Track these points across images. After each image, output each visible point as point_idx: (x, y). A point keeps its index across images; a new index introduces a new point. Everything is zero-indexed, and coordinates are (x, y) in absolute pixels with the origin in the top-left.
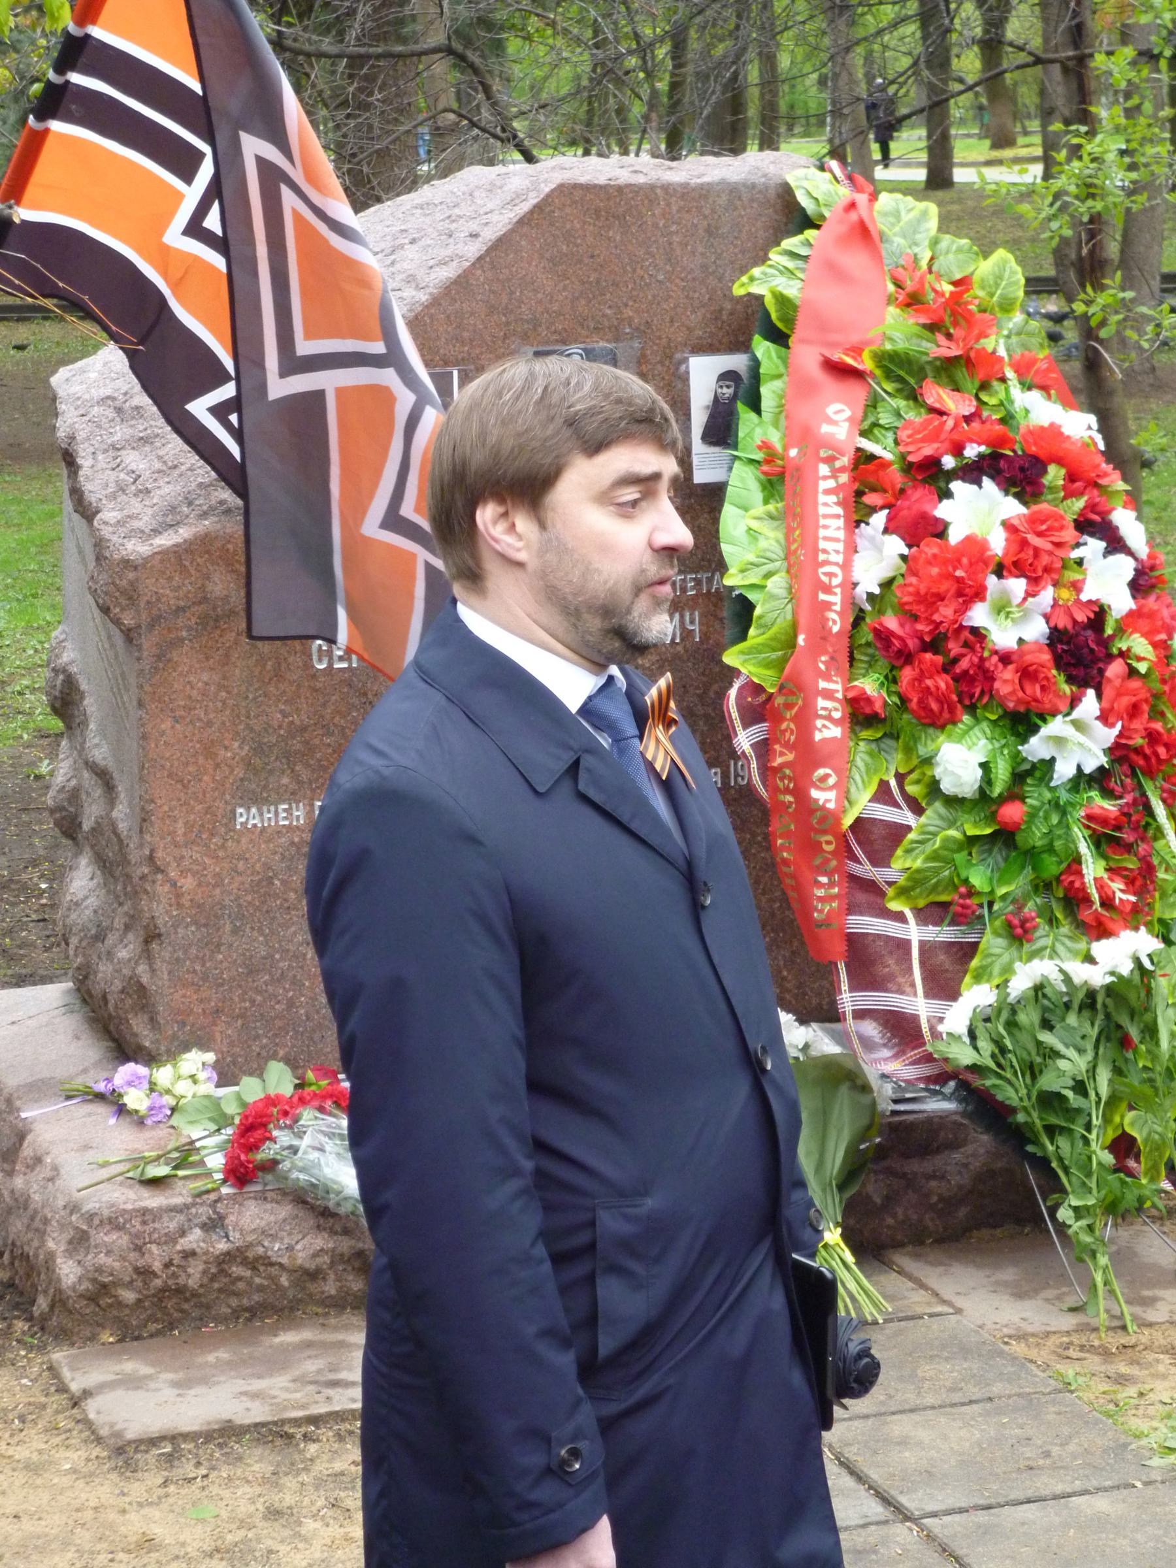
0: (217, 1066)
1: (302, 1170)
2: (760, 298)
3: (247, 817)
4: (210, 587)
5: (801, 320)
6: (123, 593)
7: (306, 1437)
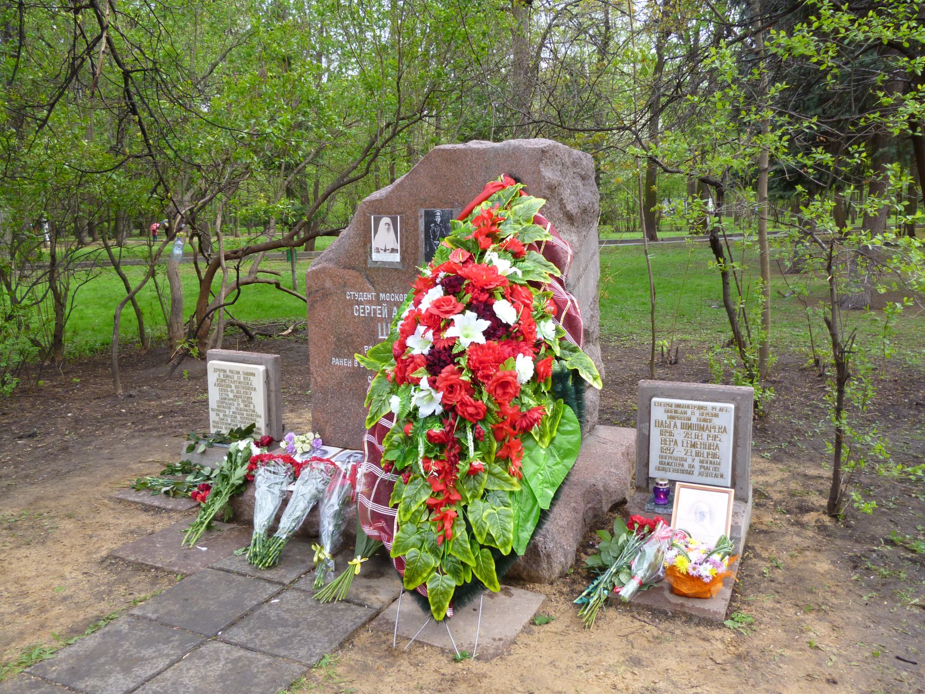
3: (336, 361)
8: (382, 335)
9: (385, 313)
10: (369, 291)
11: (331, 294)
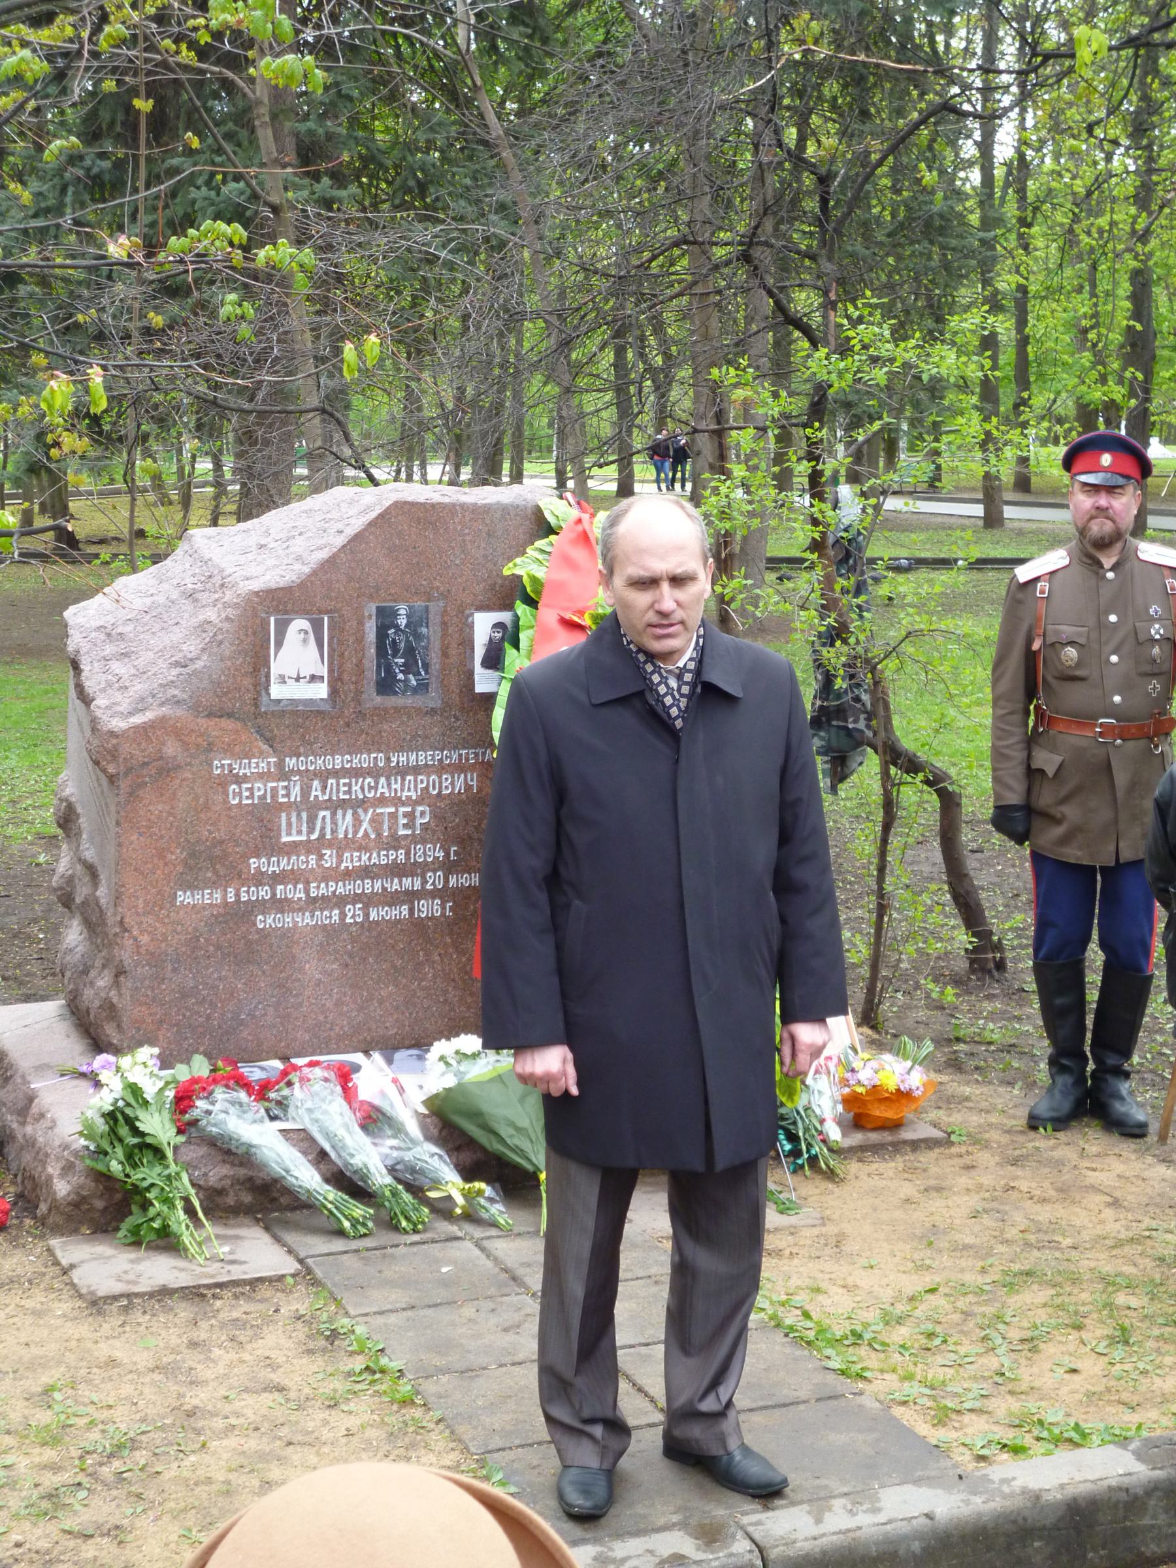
0: (159, 1057)
1: (215, 1125)
2: (520, 577)
3: (184, 898)
4: (165, 750)
5: (545, 593)
6: (109, 752)
7: (214, 1296)
8: (289, 834)
9: (296, 791)
10: (262, 755)
11: (179, 767)
